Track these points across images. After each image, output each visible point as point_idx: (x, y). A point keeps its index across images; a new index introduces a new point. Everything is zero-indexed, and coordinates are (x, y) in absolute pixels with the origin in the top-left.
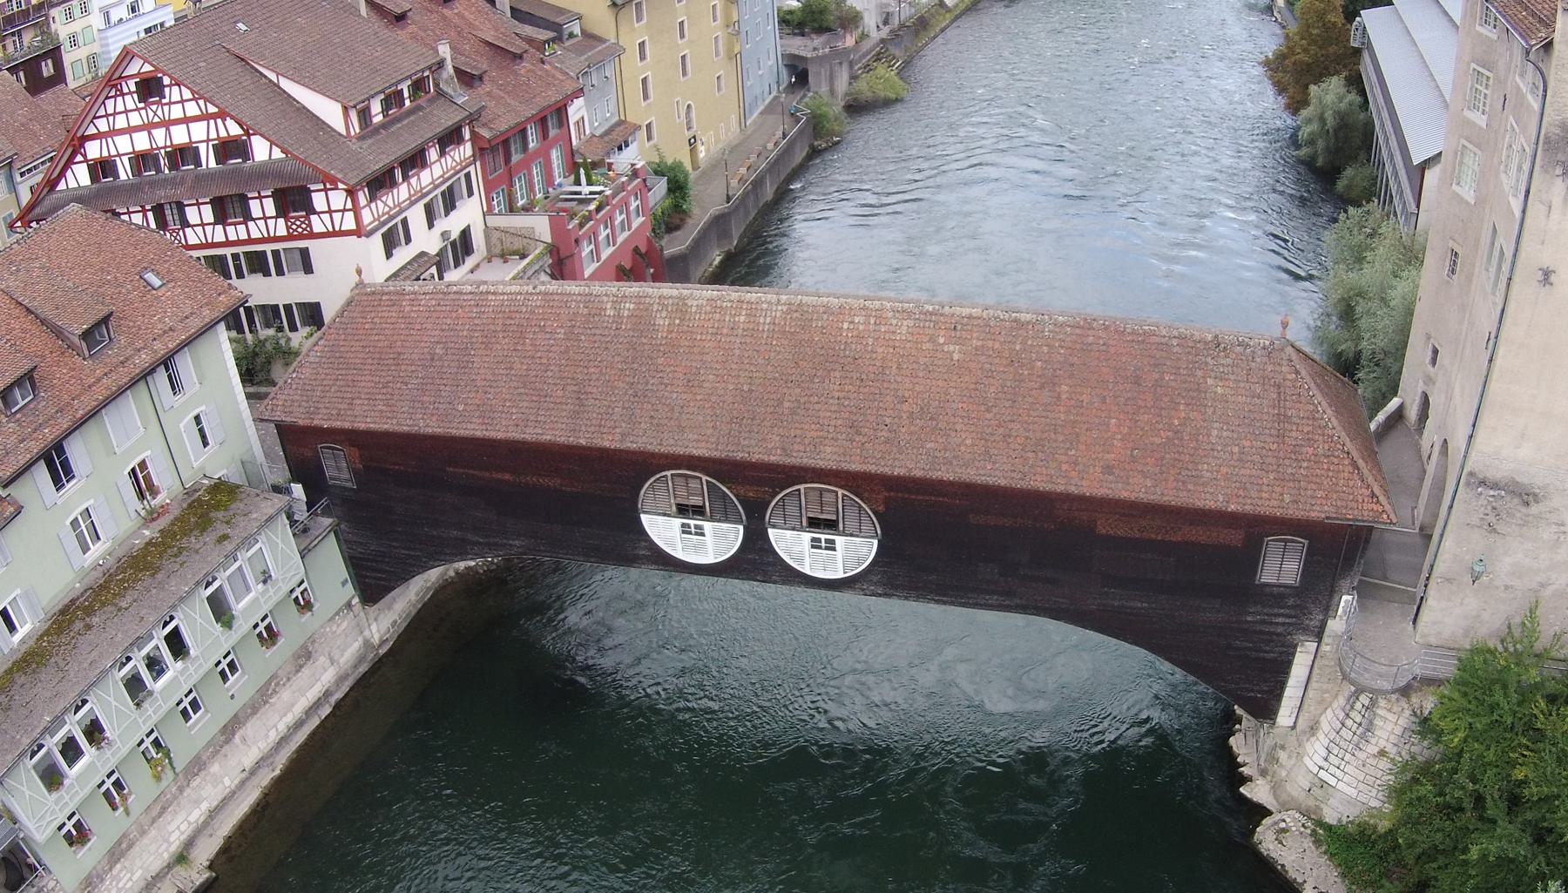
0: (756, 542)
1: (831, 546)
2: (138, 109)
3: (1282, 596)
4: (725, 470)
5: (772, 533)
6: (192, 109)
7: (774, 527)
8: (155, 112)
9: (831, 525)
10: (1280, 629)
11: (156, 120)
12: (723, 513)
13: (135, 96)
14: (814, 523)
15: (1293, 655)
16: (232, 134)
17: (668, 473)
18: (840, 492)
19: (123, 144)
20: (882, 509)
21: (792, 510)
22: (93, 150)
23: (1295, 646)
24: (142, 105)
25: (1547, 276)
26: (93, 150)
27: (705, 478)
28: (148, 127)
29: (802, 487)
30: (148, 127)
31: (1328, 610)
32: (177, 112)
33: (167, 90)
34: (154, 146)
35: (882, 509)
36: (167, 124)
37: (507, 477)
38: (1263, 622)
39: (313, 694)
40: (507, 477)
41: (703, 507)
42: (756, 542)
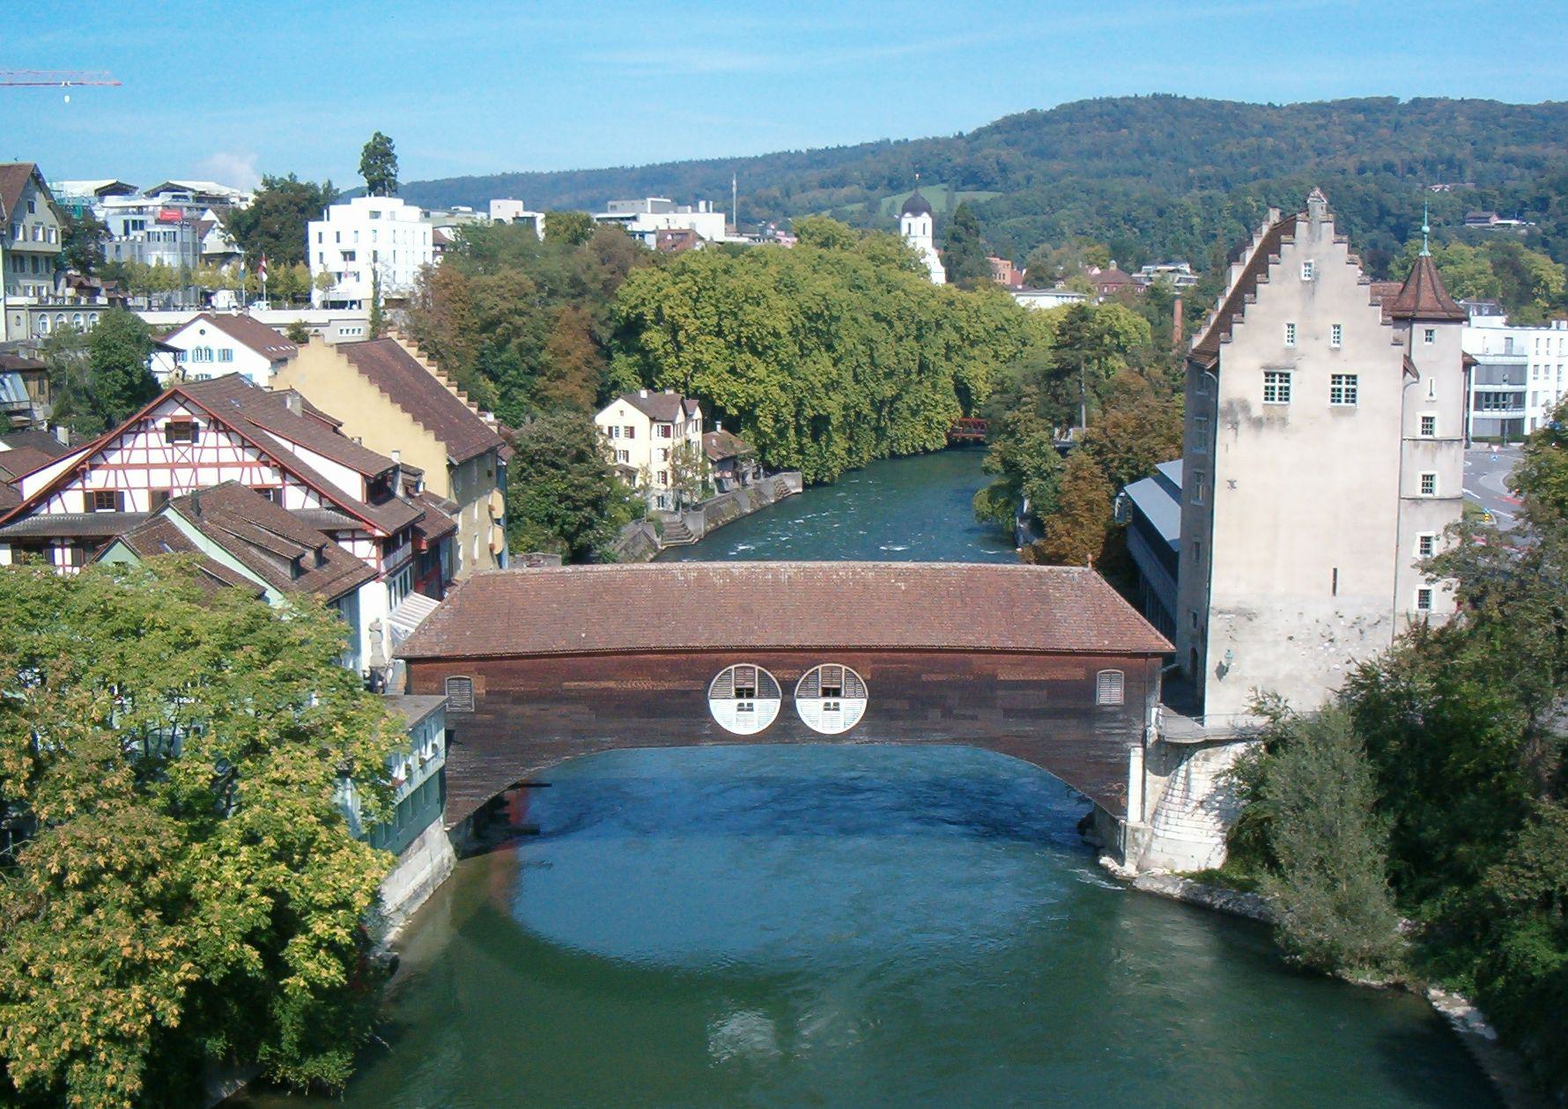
0: (788, 711)
1: (836, 707)
2: (163, 448)
3: (1114, 714)
4: (772, 656)
5: (799, 702)
6: (228, 455)
7: (800, 697)
8: (183, 451)
9: (836, 693)
10: (1117, 739)
11: (183, 460)
12: (767, 692)
13: (163, 436)
14: (826, 693)
15: (1129, 758)
16: (266, 482)
17: (733, 667)
18: (844, 668)
19: (137, 478)
20: (869, 677)
21: (812, 685)
22: (97, 480)
23: (1129, 752)
24: (170, 445)
25: (1232, 484)
26: (97, 480)
27: (757, 668)
28: (172, 467)
29: (820, 667)
30: (172, 467)
31: (1143, 718)
32: (209, 456)
33: (201, 436)
34: (175, 484)
35: (869, 677)
36: (194, 466)
37: (612, 684)
38: (1106, 734)
39: (414, 884)
40: (612, 684)
41: (753, 689)
42: (788, 711)
